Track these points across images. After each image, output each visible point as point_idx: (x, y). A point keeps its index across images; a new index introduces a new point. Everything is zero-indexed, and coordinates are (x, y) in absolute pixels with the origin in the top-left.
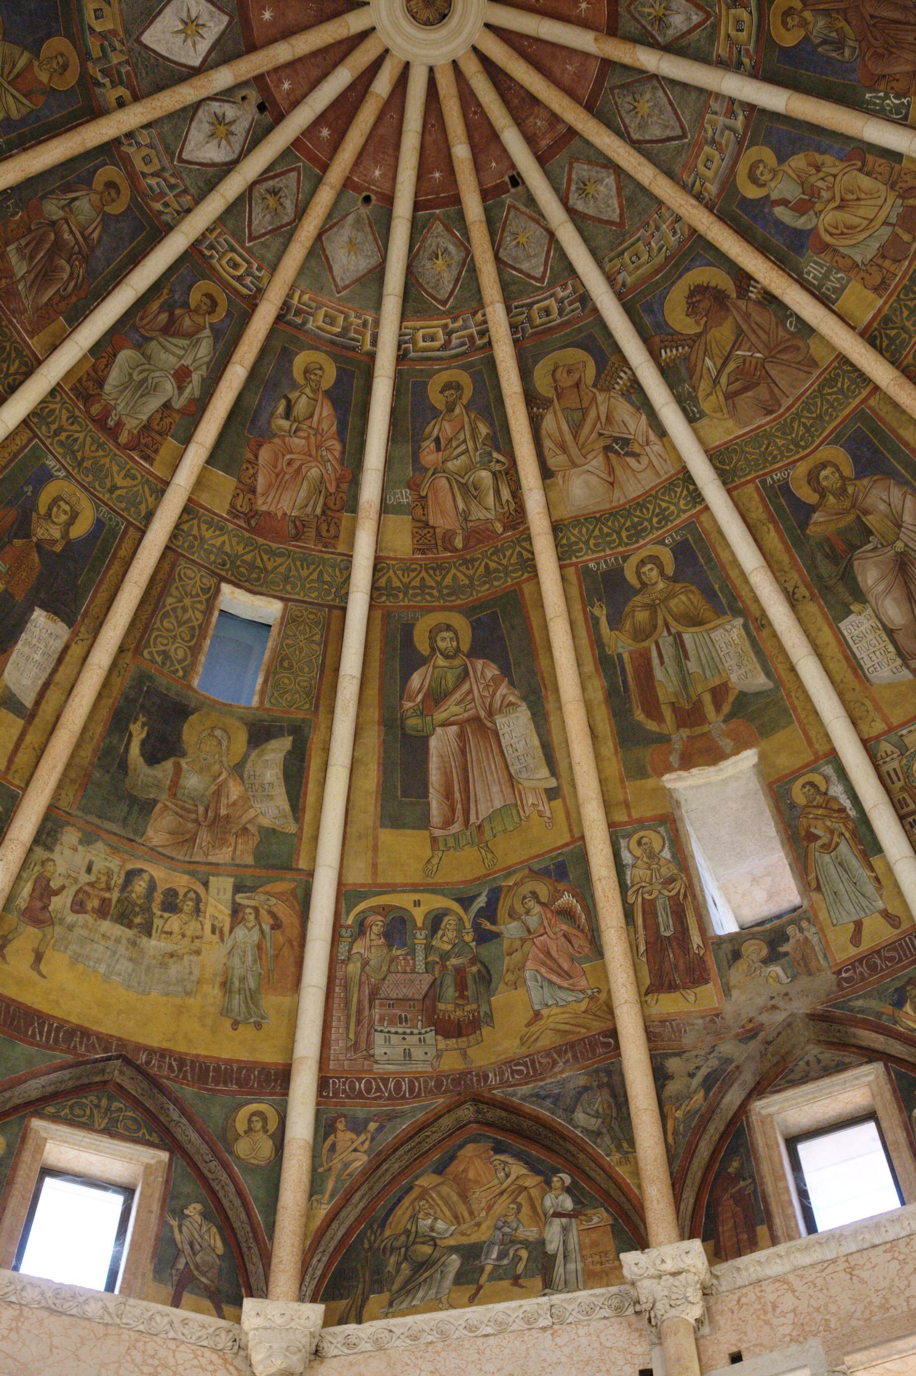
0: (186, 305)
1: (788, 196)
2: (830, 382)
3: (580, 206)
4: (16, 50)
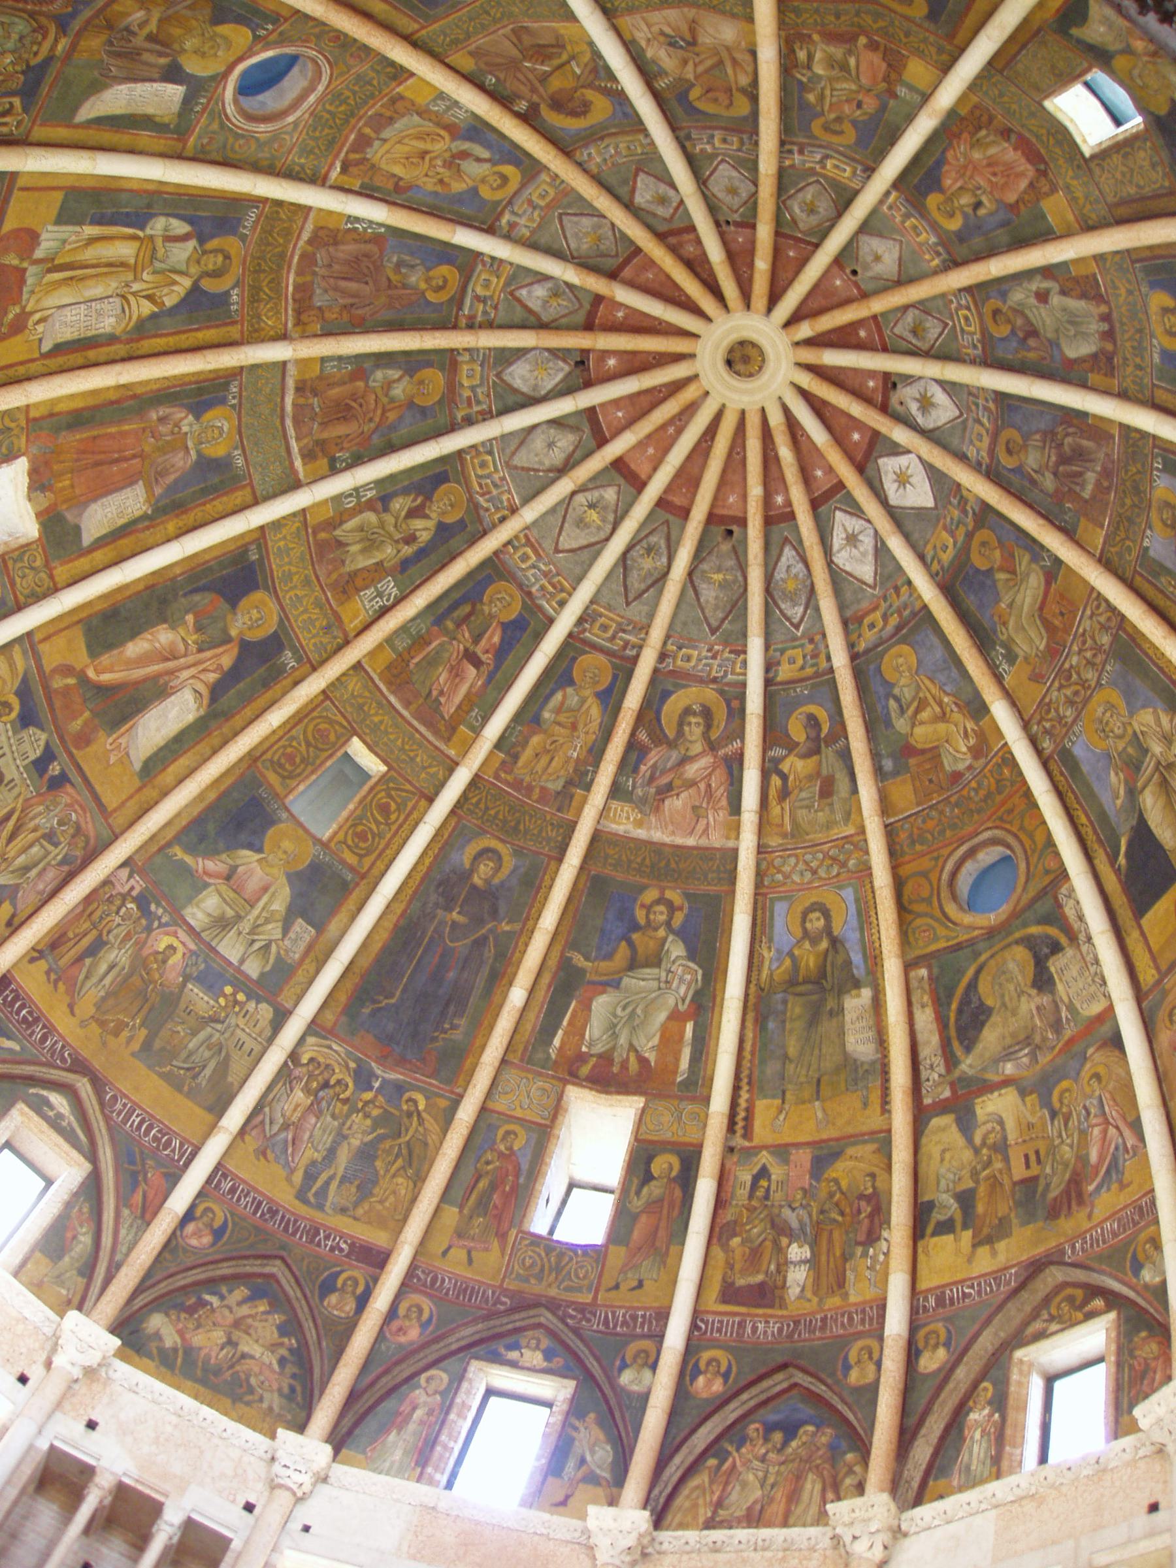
0: (1013, 332)
1: (475, 164)
2: (456, 42)
3: (671, 193)
4: (1000, 585)
